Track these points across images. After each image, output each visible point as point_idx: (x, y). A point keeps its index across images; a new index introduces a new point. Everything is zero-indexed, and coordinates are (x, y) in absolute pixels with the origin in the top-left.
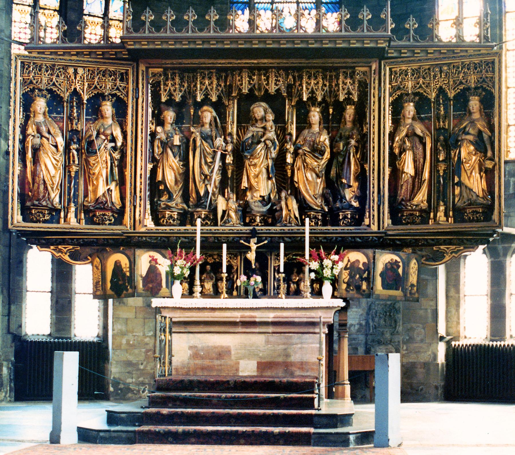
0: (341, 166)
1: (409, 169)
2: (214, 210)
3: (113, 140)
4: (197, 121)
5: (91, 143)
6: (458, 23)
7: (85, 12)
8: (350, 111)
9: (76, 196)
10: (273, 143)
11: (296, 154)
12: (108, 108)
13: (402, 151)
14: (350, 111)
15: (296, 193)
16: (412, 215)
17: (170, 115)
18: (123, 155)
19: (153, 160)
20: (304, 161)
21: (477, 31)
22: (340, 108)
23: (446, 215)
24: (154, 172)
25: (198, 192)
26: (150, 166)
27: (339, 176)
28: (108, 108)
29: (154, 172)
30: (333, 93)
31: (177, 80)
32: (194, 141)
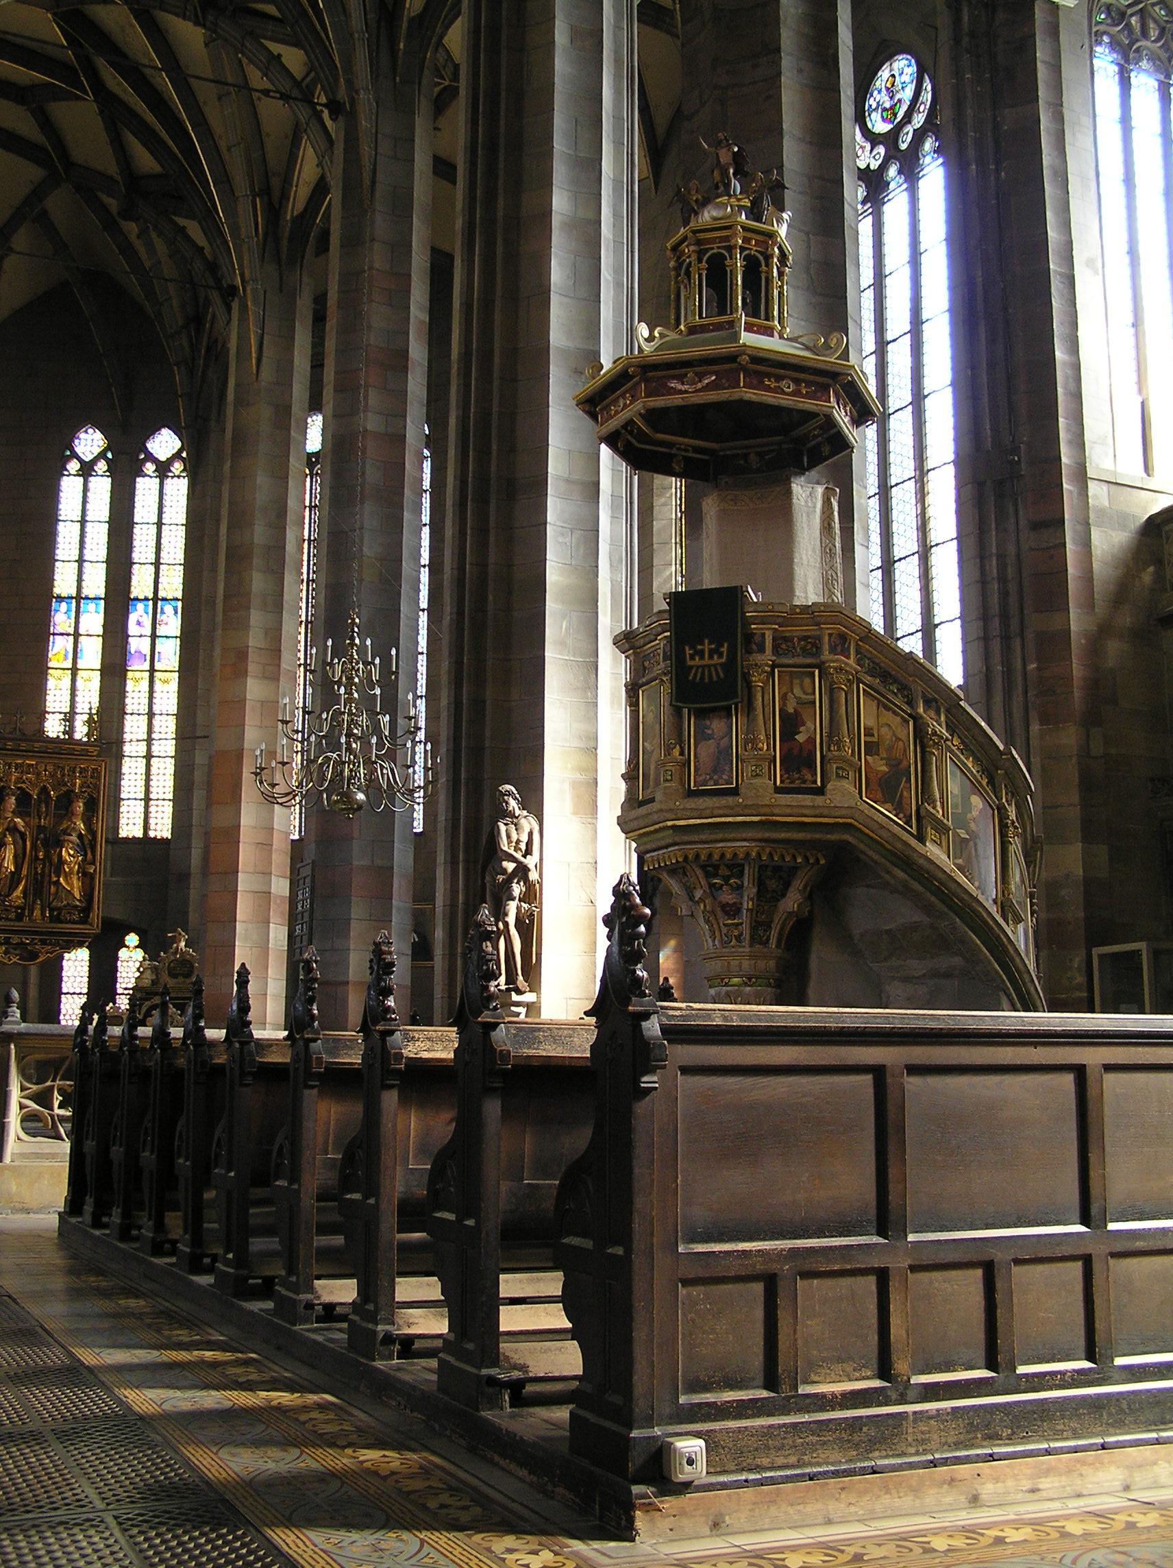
6: (70, 718)
16: (7, 910)
21: (85, 729)
23: (43, 914)
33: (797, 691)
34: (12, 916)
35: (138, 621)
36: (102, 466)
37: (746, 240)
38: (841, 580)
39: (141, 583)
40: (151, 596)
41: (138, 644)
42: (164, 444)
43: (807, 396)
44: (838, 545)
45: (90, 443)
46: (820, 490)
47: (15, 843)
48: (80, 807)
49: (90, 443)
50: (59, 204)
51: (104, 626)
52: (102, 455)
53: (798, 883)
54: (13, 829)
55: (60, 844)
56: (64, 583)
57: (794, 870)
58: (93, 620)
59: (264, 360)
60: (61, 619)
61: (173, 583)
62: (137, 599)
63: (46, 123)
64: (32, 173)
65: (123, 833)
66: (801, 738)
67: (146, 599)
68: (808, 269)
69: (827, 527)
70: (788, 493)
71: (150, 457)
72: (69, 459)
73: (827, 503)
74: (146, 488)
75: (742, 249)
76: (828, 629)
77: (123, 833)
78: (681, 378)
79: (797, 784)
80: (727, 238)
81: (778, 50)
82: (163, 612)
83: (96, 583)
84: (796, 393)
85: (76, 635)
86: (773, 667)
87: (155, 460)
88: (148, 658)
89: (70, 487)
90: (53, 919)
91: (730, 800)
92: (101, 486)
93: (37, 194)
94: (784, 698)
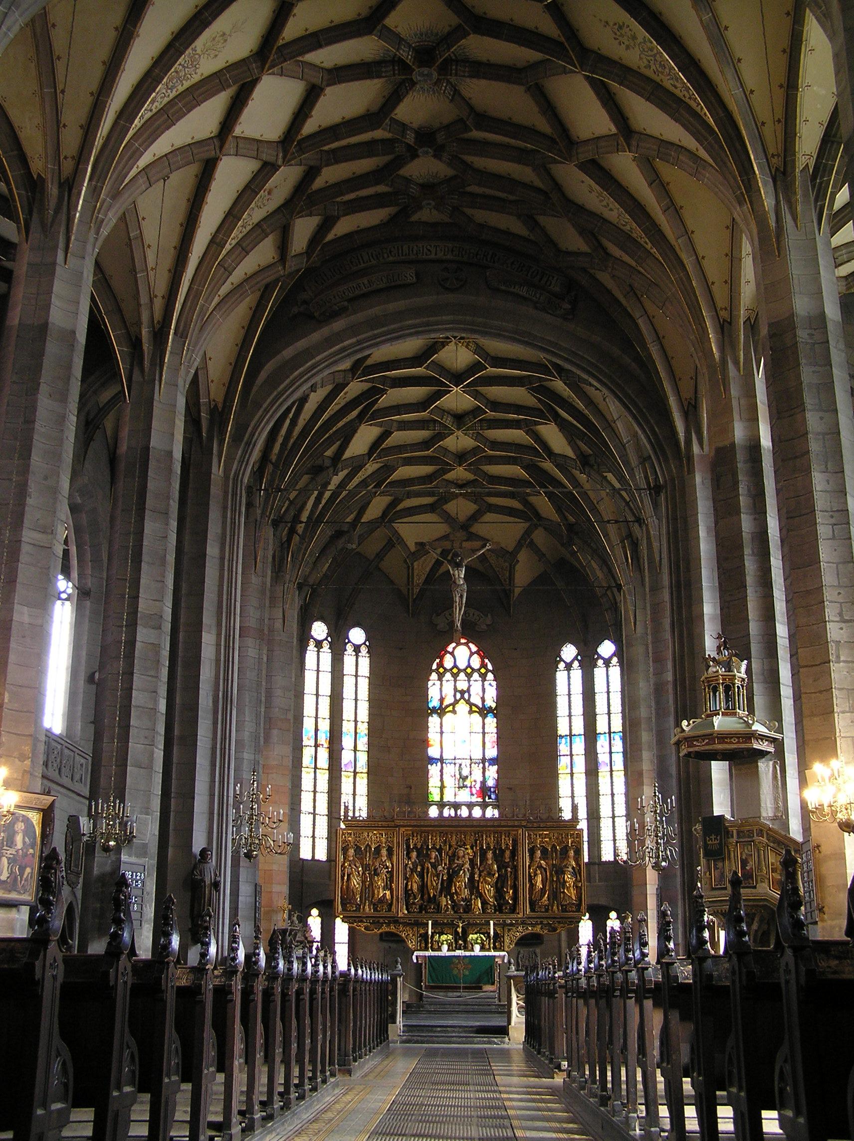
0: (503, 882)
1: (539, 885)
2: (438, 905)
3: (387, 868)
4: (428, 856)
5: (375, 870)
7: (343, 770)
8: (508, 853)
9: (369, 897)
10: (468, 870)
11: (480, 875)
12: (384, 852)
13: (536, 875)
14: (508, 853)
15: (480, 896)
17: (414, 854)
18: (392, 876)
19: (406, 878)
20: (484, 879)
22: (502, 852)
23: (558, 908)
24: (407, 884)
25: (429, 895)
26: (405, 882)
27: (503, 887)
28: (384, 852)
29: (407, 884)
30: (498, 843)
31: (419, 837)
32: (428, 868)
33: (746, 851)
34: (543, 910)
35: (602, 745)
36: (576, 664)
37: (723, 679)
38: (781, 797)
39: (601, 725)
40: (607, 731)
41: (603, 757)
42: (607, 648)
43: (743, 743)
44: (779, 783)
45: (569, 652)
46: (771, 763)
47: (541, 873)
48: (572, 853)
49: (569, 652)
50: (539, 537)
51: (585, 750)
52: (576, 658)
53: (756, 919)
54: (540, 867)
55: (563, 873)
56: (562, 728)
57: (754, 914)
58: (579, 746)
59: (638, 623)
60: (563, 748)
61: (617, 724)
62: (600, 734)
63: (526, 503)
64: (522, 526)
65: (603, 859)
66: (748, 868)
67: (605, 733)
68: (763, 674)
69: (775, 777)
70: (757, 766)
71: (600, 657)
72: (559, 662)
73: (775, 768)
74: (599, 673)
75: (723, 683)
76: (755, 828)
77: (603, 859)
78: (697, 741)
79: (747, 885)
80: (716, 680)
81: (746, 586)
82: (614, 739)
83: (579, 726)
84: (738, 742)
85: (571, 755)
86: (737, 842)
87: (603, 658)
88: (609, 764)
89: (561, 676)
90: (564, 910)
91: (723, 892)
92: (577, 674)
93: (528, 533)
94: (741, 854)
